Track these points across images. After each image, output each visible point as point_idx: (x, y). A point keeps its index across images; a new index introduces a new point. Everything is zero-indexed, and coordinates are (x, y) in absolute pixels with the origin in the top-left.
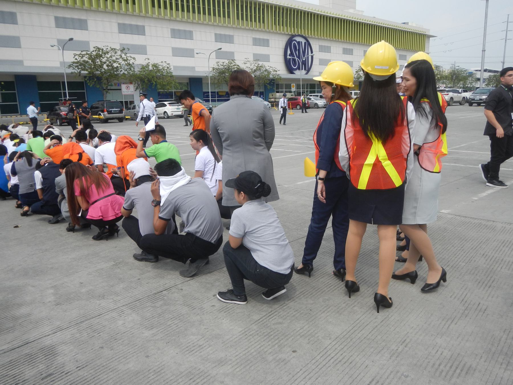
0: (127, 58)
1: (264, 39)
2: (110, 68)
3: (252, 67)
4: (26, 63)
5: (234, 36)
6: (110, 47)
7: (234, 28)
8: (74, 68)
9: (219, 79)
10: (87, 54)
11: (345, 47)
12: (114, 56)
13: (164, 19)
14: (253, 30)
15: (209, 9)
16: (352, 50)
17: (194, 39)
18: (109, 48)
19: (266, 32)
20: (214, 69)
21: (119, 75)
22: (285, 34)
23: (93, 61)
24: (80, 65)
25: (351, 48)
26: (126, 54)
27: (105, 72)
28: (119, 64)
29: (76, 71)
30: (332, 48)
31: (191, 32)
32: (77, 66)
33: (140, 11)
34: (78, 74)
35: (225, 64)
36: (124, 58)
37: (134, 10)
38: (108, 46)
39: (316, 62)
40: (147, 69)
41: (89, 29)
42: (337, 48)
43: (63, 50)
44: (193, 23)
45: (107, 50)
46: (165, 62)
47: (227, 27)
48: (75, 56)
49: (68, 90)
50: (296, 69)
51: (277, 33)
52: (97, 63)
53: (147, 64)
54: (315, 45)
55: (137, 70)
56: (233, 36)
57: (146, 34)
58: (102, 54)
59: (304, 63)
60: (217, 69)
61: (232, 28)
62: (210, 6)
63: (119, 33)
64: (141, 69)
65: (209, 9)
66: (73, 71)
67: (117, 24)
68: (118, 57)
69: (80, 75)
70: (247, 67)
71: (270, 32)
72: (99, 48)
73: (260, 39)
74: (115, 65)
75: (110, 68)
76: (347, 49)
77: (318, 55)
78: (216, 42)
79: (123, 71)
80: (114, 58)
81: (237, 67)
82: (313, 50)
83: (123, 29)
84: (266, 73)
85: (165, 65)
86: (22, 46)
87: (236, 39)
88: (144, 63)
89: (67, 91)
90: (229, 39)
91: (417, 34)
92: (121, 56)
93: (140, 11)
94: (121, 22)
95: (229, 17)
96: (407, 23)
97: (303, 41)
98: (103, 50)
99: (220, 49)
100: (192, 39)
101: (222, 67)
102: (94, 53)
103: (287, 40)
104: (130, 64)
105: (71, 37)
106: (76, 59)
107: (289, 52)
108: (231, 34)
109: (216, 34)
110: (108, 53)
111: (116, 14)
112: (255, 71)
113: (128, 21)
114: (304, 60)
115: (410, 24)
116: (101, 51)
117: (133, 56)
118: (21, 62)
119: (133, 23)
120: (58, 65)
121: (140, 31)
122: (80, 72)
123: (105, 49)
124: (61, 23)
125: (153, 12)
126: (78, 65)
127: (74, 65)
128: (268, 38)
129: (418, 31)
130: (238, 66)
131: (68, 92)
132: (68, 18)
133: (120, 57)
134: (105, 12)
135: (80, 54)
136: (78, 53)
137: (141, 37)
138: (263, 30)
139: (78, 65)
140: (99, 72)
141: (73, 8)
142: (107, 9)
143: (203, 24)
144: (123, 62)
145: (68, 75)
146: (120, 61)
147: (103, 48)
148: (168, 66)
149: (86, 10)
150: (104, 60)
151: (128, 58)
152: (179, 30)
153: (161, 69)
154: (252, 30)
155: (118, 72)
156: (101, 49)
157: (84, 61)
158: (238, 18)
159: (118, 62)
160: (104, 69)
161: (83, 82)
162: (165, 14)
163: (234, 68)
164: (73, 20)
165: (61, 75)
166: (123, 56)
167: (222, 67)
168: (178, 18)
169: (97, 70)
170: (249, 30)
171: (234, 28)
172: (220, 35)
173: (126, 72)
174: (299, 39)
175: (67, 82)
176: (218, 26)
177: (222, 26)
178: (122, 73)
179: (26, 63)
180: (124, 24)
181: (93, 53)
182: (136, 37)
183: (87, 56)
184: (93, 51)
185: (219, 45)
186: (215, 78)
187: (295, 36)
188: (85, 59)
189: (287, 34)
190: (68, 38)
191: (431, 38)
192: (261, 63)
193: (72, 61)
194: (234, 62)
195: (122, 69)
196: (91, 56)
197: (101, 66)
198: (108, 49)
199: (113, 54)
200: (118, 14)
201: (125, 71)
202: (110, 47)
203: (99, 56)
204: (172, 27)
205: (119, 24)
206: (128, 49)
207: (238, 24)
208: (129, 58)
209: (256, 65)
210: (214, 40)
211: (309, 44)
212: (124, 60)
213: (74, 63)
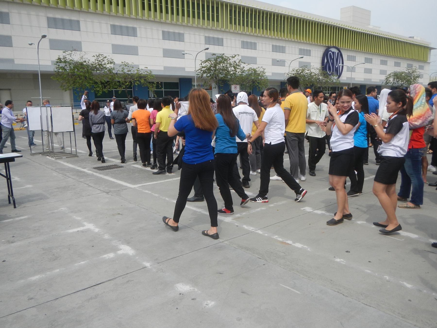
1: (307, 50)
5: (286, 47)
11: (367, 57)
13: (238, 33)
14: (300, 42)
16: (372, 59)
19: (309, 44)
22: (323, 46)
25: (371, 58)
30: (357, 57)
31: (255, 44)
33: (222, 26)
37: (218, 26)
39: (345, 68)
42: (360, 58)
44: (257, 36)
46: (262, 67)
47: (282, 40)
50: (330, 75)
51: (317, 45)
54: (345, 55)
56: (285, 47)
57: (224, 45)
59: (337, 70)
61: (286, 40)
63: (205, 44)
67: (204, 36)
71: (311, 44)
73: (304, 50)
76: (368, 58)
77: (347, 63)
78: (273, 51)
82: (344, 59)
83: (208, 41)
86: (139, 54)
90: (282, 50)
91: (422, 46)
94: (207, 35)
96: (413, 37)
97: (336, 51)
103: (324, 51)
107: (326, 61)
108: (284, 45)
109: (273, 45)
111: (204, 29)
114: (337, 67)
115: (415, 38)
119: (216, 36)
120: (163, 69)
121: (219, 42)
124: (167, 36)
128: (310, 49)
129: (422, 44)
134: (197, 28)
137: (220, 47)
141: (176, 25)
143: (265, 37)
149: (184, 26)
152: (247, 42)
161: (178, 83)
170: (298, 42)
172: (276, 46)
174: (333, 50)
180: (209, 37)
187: (331, 47)
189: (324, 46)
191: (432, 51)
200: (206, 29)
204: (242, 40)
205: (205, 37)
210: (271, 50)
211: (341, 55)
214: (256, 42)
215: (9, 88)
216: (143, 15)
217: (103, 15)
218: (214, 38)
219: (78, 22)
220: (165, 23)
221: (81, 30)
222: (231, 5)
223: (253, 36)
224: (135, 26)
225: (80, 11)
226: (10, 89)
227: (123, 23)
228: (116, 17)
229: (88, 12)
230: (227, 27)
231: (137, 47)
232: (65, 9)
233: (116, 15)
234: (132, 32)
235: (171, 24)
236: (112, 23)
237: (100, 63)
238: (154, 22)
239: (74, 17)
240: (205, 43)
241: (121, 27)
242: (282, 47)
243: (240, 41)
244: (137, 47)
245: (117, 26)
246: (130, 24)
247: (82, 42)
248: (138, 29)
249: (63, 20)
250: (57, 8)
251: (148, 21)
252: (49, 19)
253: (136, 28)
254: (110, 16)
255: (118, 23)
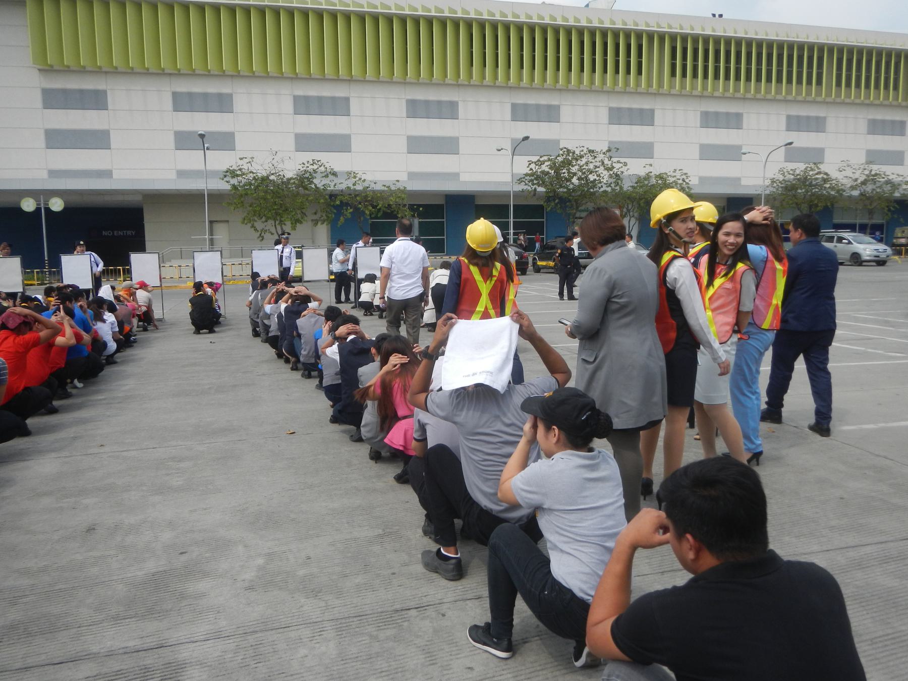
0: (612, 165)
1: (893, 122)
2: (583, 182)
3: (856, 176)
4: (464, 177)
6: (587, 148)
7: (827, 103)
8: (527, 183)
9: (784, 200)
10: (549, 160)
12: (591, 162)
13: (691, 96)
15: (780, 73)
17: (745, 125)
18: (585, 150)
20: (773, 181)
21: (597, 194)
23: (557, 172)
24: (536, 179)
26: (611, 157)
27: (574, 190)
28: (599, 176)
29: (529, 188)
31: (739, 116)
32: (532, 181)
33: (650, 84)
34: (532, 193)
35: (798, 172)
36: (607, 165)
37: (638, 84)
38: (583, 147)
40: (646, 182)
41: (561, 121)
43: (513, 155)
44: (744, 99)
45: (582, 153)
46: (680, 170)
47: (814, 102)
48: (530, 164)
49: (513, 218)
52: (562, 175)
53: (647, 174)
55: (627, 185)
56: (825, 118)
57: (656, 123)
58: (572, 159)
60: (780, 182)
62: (782, 66)
64: (636, 183)
65: (780, 73)
66: (525, 187)
67: (607, 109)
68: (598, 164)
69: (535, 195)
70: (847, 177)
72: (568, 151)
74: (592, 177)
75: (583, 182)
79: (604, 188)
80: (591, 166)
81: (823, 177)
83: (617, 117)
84: (888, 188)
85: (678, 174)
87: (831, 124)
88: (642, 173)
89: (512, 220)
92: (603, 163)
93: (650, 84)
95: (819, 82)
98: (574, 153)
99: (791, 143)
100: (739, 126)
101: (792, 177)
102: (560, 159)
104: (617, 175)
105: (526, 135)
106: (531, 169)
108: (822, 115)
109: (789, 117)
110: (581, 157)
112: (864, 183)
113: (626, 103)
116: (571, 154)
117: (622, 160)
118: (457, 175)
120: (508, 178)
121: (645, 118)
122: (535, 189)
123: (577, 152)
125: (672, 86)
126: (533, 178)
127: (526, 178)
130: (826, 174)
131: (513, 222)
132: (532, 105)
133: (601, 163)
134: (591, 91)
135: (539, 161)
136: (535, 159)
138: (895, 103)
139: (533, 178)
140: (565, 190)
141: (542, 89)
142: (593, 86)
144: (605, 172)
145: (517, 195)
146: (601, 170)
147: (575, 149)
148: (684, 177)
149: (560, 90)
150: (574, 169)
151: (614, 164)
153: (672, 183)
154: (868, 105)
155: (595, 190)
156: (571, 153)
157: (543, 172)
158: (839, 84)
159: (596, 172)
160: (573, 184)
162: (694, 87)
163: (817, 179)
164: (538, 107)
165: (506, 195)
166: (606, 161)
167: (792, 177)
168: (717, 92)
169: (561, 187)
170: (862, 104)
171: (827, 103)
173: (609, 189)
175: (514, 205)
176: (795, 101)
177: (805, 102)
178: (602, 190)
179: (464, 177)
180: (619, 109)
181: (558, 158)
182: (637, 129)
183: (548, 163)
184: (559, 156)
185: (793, 136)
186: (775, 199)
188: (545, 168)
190: (521, 136)
192: (875, 168)
193: (525, 173)
194: (818, 168)
195: (602, 184)
196: (554, 164)
197: (569, 180)
198: (583, 151)
199: (590, 159)
201: (607, 187)
202: (587, 148)
203: (567, 163)
205: (611, 110)
206: (616, 150)
207: (838, 95)
208: (617, 166)
209: (867, 172)
212: (608, 169)
213: (526, 175)
214: (741, 111)
215: (226, 220)
216: (470, 76)
217: (391, 82)
218: (630, 110)
219: (347, 100)
220: (518, 88)
221: (351, 115)
222: (673, 37)
223: (733, 98)
224: (455, 99)
225: (351, 80)
226: (228, 221)
227: (432, 95)
228: (418, 83)
229: (364, 81)
230: (660, 84)
231: (458, 138)
232: (323, 79)
233: (415, 81)
234: (449, 111)
235: (531, 89)
236: (409, 97)
237: (307, 175)
238: (494, 87)
239: (339, 91)
240: (608, 123)
241: (427, 102)
242: (817, 118)
243: (699, 113)
244: (458, 138)
245: (420, 101)
246: (445, 96)
247: (353, 137)
248: (461, 105)
249: (320, 99)
250: (309, 78)
251: (482, 86)
252: (296, 99)
253: (457, 103)
254: (404, 83)
255: (420, 95)
